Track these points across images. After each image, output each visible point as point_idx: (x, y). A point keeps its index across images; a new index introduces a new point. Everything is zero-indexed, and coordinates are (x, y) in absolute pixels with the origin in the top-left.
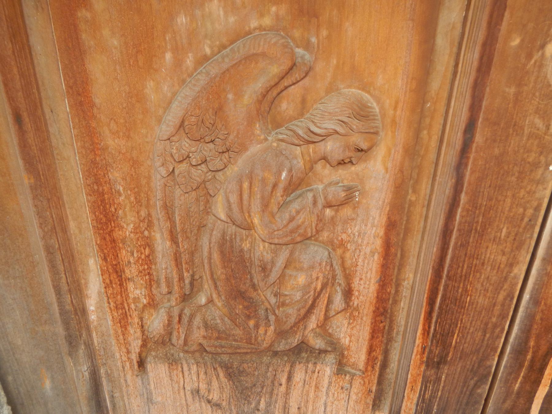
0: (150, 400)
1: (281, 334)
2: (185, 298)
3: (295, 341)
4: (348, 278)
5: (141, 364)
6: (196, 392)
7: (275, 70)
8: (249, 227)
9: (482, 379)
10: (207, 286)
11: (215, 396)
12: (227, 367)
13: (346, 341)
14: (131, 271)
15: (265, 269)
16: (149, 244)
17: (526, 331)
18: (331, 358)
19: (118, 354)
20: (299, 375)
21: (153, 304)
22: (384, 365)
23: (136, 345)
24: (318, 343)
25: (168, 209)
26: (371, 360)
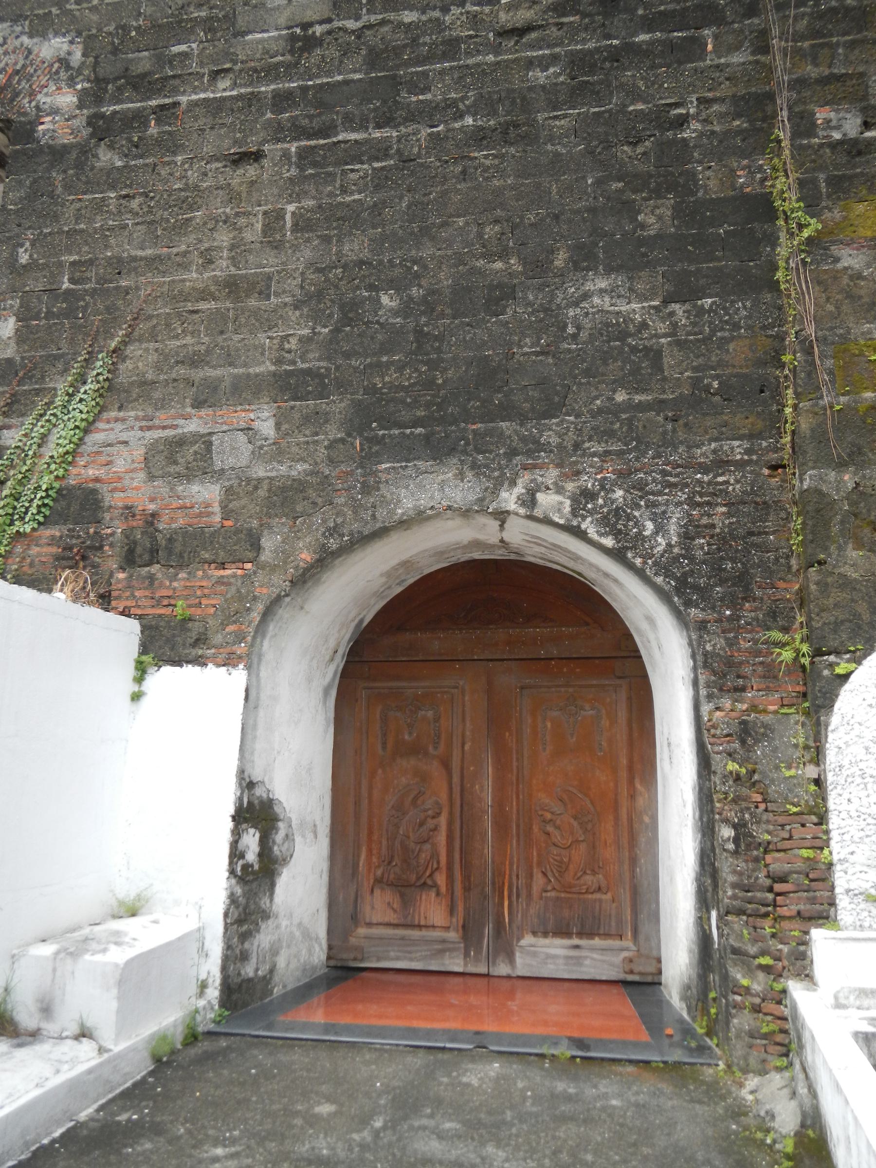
0: (373, 908)
1: (418, 878)
2: (390, 863)
3: (422, 881)
4: (438, 856)
5: (372, 891)
6: (389, 904)
7: (416, 792)
8: (408, 837)
9: (485, 898)
10: (396, 857)
11: (395, 906)
12: (400, 892)
13: (439, 882)
14: (374, 852)
15: (413, 852)
16: (381, 843)
17: (493, 874)
18: (434, 889)
19: (365, 884)
20: (424, 897)
21: (379, 866)
22: (453, 893)
23: (372, 881)
24: (429, 882)
25: (387, 831)
26: (447, 889)
